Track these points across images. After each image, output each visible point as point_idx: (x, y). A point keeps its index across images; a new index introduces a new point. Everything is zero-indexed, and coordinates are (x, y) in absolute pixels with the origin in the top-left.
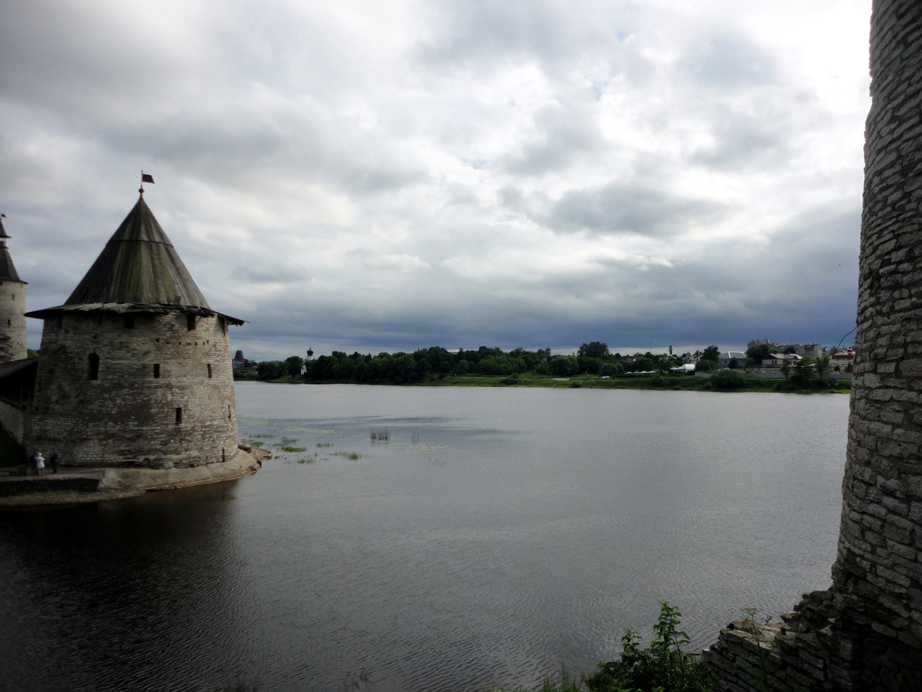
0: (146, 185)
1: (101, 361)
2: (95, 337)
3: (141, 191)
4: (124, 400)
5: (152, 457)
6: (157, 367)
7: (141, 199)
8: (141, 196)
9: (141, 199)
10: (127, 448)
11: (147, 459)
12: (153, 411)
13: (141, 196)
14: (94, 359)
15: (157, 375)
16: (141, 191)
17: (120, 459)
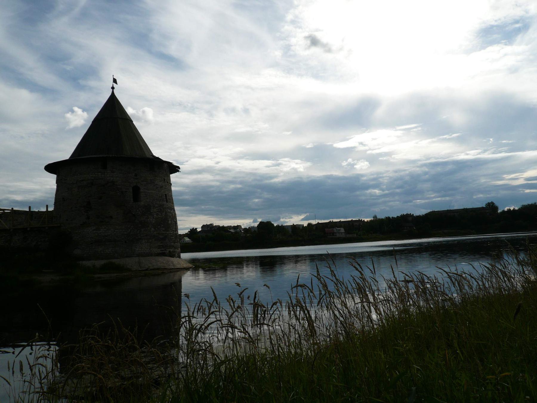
0: (115, 85)
1: (141, 190)
2: (136, 175)
3: (113, 88)
4: (157, 214)
5: (171, 250)
6: (166, 195)
7: (113, 94)
8: (113, 92)
9: (113, 94)
10: (161, 244)
11: (170, 251)
12: (170, 222)
13: (113, 92)
14: (136, 190)
15: (167, 201)
16: (113, 88)
17: (159, 251)
